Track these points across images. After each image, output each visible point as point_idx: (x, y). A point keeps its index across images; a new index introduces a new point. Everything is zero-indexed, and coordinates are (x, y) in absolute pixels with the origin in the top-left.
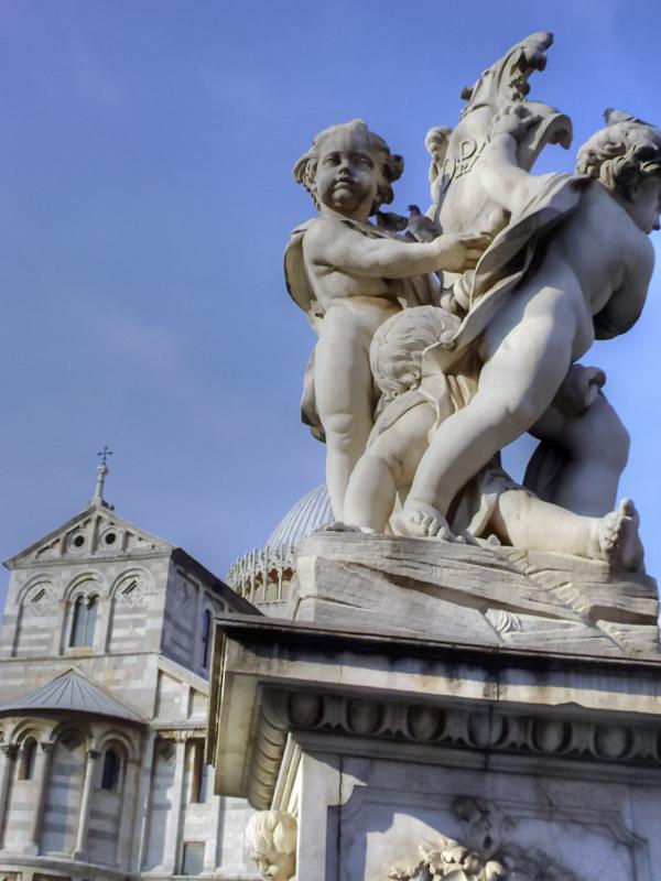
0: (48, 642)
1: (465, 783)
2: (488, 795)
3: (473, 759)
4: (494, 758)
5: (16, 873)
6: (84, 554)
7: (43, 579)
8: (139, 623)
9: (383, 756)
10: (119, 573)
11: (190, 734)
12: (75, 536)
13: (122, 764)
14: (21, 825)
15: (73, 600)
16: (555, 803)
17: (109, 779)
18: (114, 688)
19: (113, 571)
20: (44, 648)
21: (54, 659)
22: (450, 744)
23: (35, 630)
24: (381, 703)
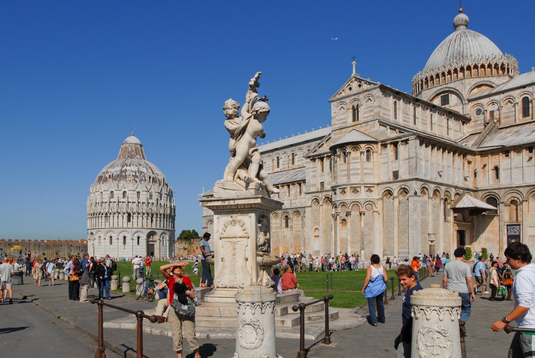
0: (346, 122)
5: (345, 188)
6: (352, 92)
7: (341, 103)
8: (371, 111)
10: (363, 97)
11: (391, 141)
12: (349, 87)
13: (372, 153)
14: (344, 175)
15: (351, 107)
17: (368, 159)
18: (366, 132)
19: (361, 96)
20: (345, 124)
21: (348, 127)
22: (222, 210)
23: (341, 119)
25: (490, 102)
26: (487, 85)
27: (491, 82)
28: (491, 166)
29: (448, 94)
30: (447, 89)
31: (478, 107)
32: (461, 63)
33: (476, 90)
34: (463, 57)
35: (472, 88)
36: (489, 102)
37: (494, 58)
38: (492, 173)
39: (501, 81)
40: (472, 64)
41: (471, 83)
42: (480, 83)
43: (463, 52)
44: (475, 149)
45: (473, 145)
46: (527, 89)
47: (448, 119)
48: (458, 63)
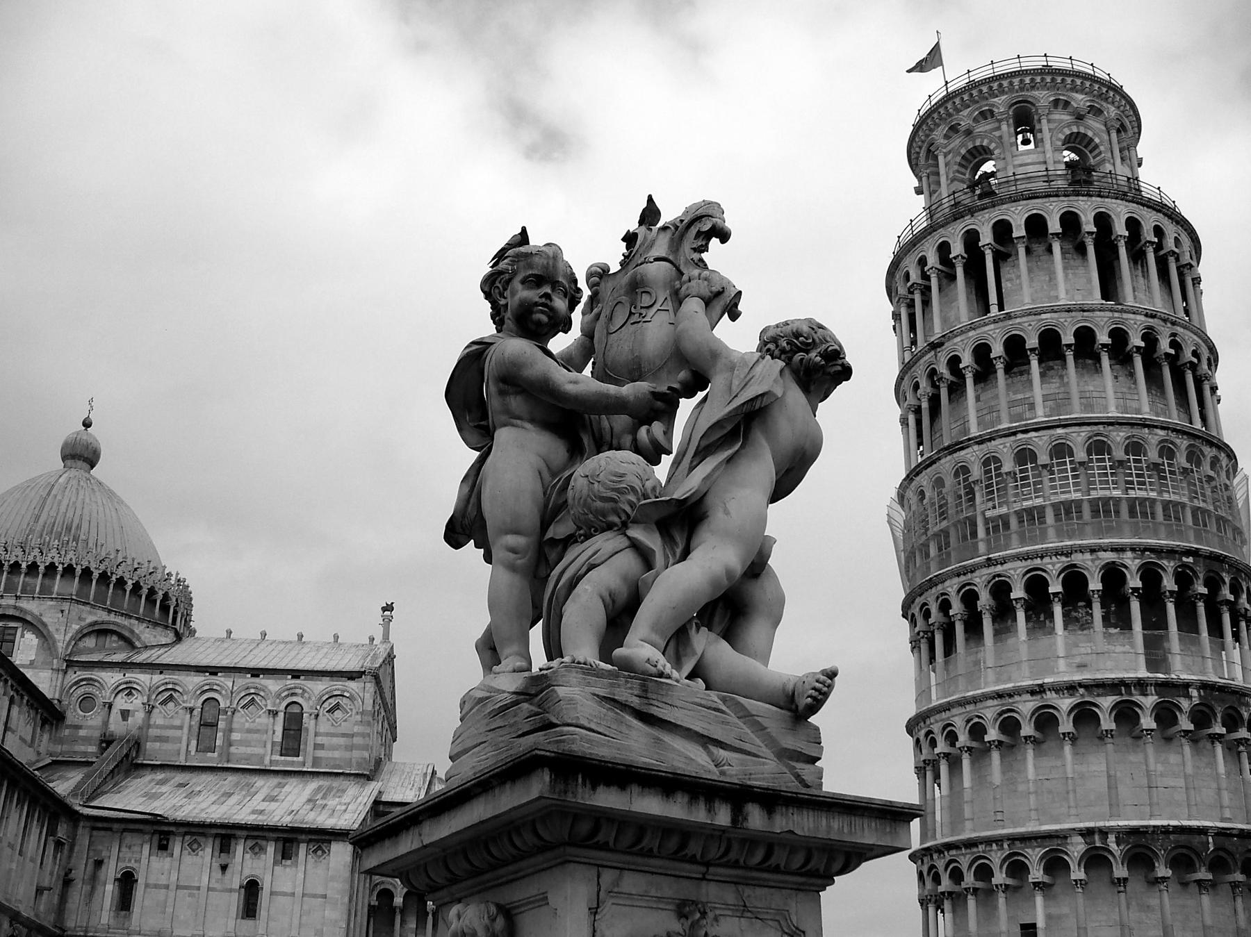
1: (686, 890)
2: (704, 900)
3: (696, 870)
4: (712, 869)
9: (633, 867)
16: (747, 904)
24: (643, 825)
25: (125, 686)
26: (121, 637)
27: (132, 632)
28: (111, 871)
29: (16, 628)
30: (17, 614)
31: (81, 691)
32: (71, 555)
33: (90, 642)
34: (76, 539)
35: (85, 631)
36: (120, 684)
37: (150, 574)
38: (109, 890)
39: (155, 637)
40: (96, 568)
41: (84, 616)
42: (111, 627)
43: (79, 527)
44: (77, 805)
45: (74, 792)
46: (220, 679)
47: (12, 701)
48: (63, 553)
